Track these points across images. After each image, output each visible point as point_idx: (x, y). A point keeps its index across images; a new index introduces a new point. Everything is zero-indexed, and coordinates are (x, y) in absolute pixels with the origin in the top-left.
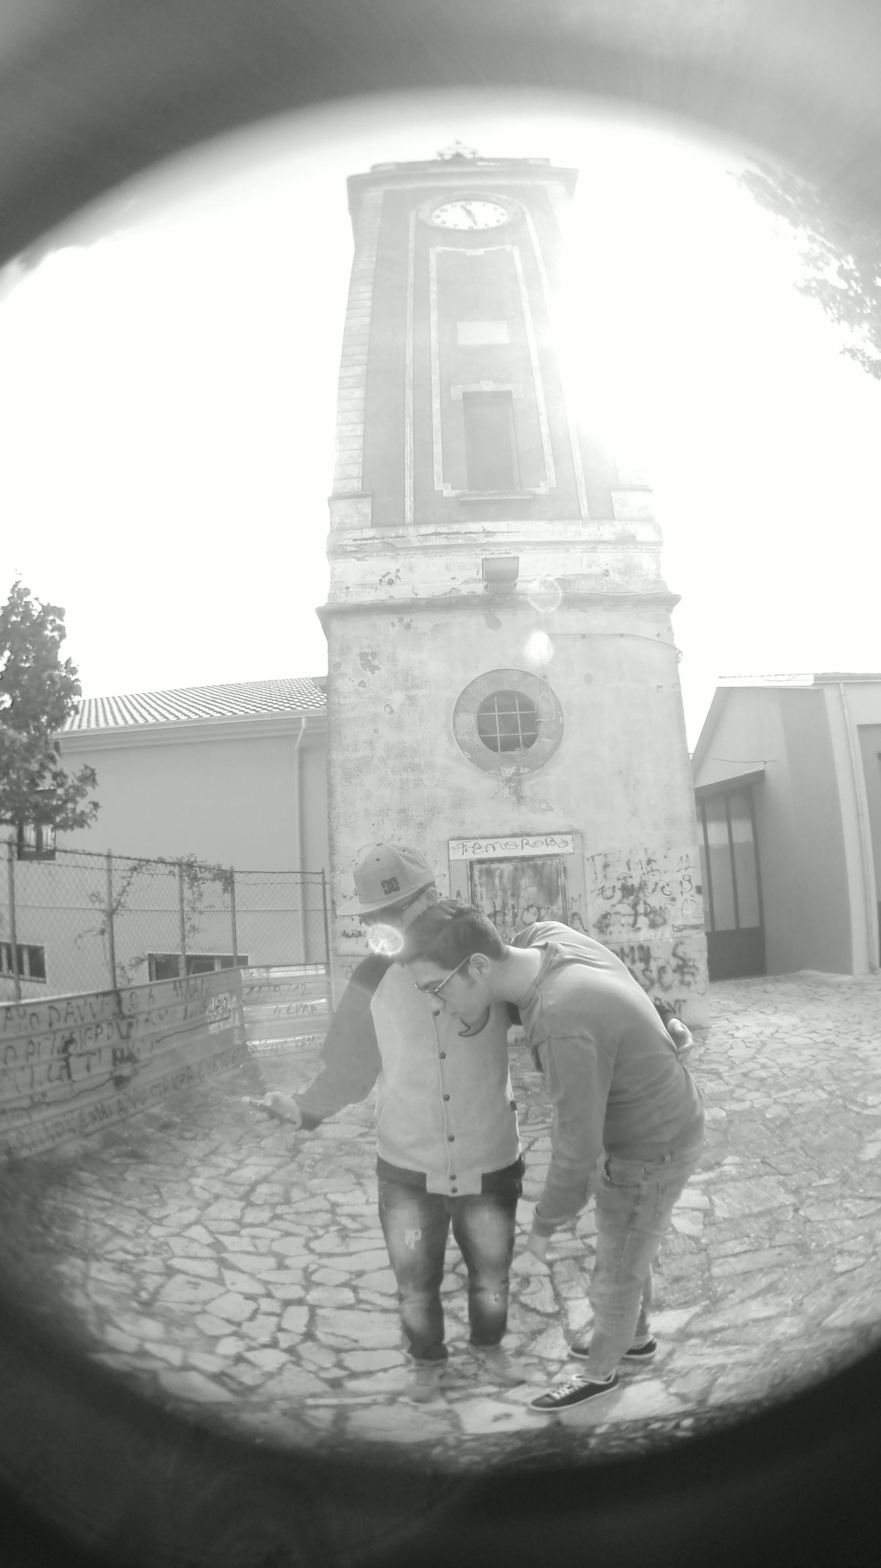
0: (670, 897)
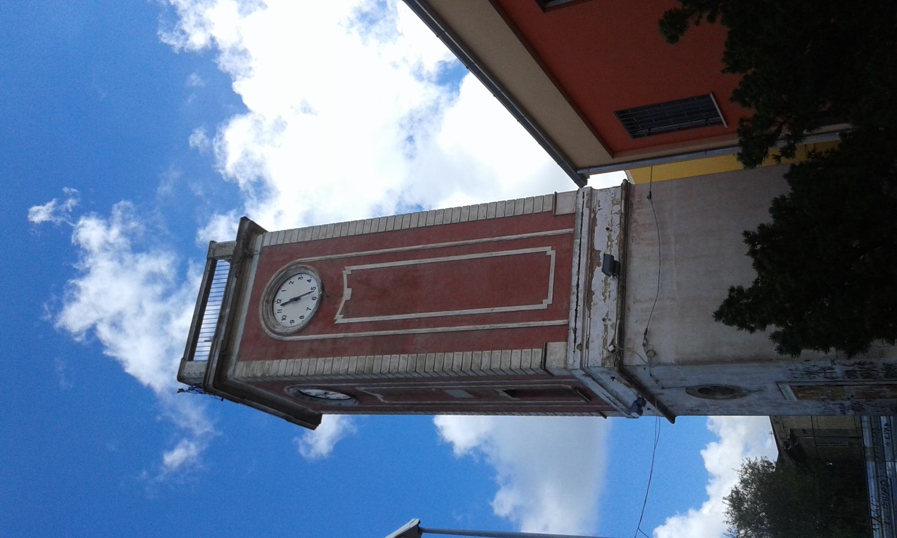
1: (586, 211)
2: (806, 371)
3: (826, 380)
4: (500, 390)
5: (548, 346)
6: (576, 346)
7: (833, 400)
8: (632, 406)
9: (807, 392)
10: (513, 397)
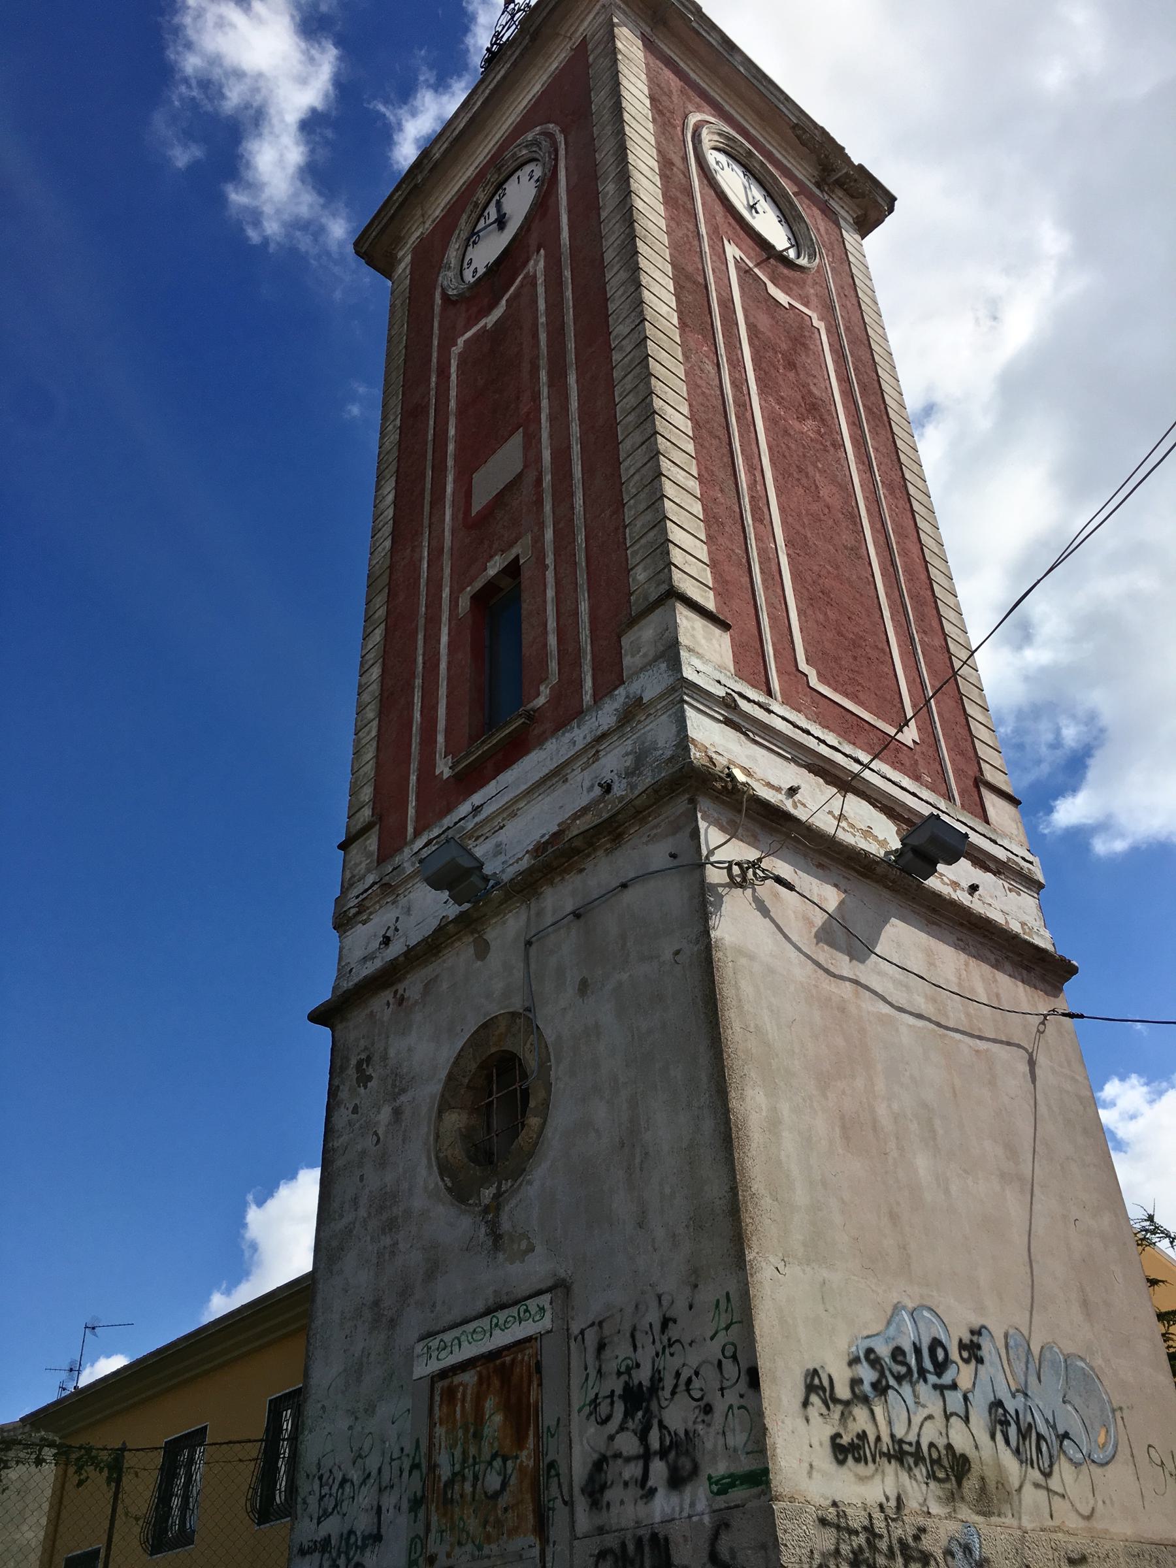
0: (702, 1403)
1: (1001, 855)
2: (657, 1379)
3: (580, 1469)
4: (514, 552)
5: (717, 632)
6: (733, 693)
7: (416, 1504)
8: (471, 855)
9: (489, 1404)
10: (475, 598)
